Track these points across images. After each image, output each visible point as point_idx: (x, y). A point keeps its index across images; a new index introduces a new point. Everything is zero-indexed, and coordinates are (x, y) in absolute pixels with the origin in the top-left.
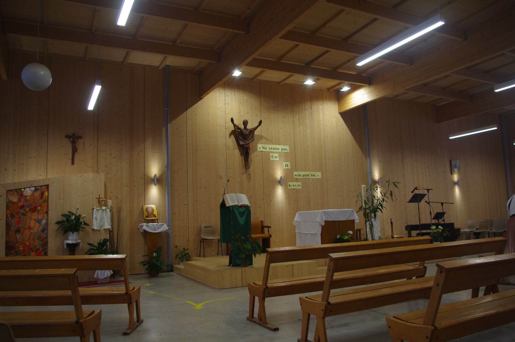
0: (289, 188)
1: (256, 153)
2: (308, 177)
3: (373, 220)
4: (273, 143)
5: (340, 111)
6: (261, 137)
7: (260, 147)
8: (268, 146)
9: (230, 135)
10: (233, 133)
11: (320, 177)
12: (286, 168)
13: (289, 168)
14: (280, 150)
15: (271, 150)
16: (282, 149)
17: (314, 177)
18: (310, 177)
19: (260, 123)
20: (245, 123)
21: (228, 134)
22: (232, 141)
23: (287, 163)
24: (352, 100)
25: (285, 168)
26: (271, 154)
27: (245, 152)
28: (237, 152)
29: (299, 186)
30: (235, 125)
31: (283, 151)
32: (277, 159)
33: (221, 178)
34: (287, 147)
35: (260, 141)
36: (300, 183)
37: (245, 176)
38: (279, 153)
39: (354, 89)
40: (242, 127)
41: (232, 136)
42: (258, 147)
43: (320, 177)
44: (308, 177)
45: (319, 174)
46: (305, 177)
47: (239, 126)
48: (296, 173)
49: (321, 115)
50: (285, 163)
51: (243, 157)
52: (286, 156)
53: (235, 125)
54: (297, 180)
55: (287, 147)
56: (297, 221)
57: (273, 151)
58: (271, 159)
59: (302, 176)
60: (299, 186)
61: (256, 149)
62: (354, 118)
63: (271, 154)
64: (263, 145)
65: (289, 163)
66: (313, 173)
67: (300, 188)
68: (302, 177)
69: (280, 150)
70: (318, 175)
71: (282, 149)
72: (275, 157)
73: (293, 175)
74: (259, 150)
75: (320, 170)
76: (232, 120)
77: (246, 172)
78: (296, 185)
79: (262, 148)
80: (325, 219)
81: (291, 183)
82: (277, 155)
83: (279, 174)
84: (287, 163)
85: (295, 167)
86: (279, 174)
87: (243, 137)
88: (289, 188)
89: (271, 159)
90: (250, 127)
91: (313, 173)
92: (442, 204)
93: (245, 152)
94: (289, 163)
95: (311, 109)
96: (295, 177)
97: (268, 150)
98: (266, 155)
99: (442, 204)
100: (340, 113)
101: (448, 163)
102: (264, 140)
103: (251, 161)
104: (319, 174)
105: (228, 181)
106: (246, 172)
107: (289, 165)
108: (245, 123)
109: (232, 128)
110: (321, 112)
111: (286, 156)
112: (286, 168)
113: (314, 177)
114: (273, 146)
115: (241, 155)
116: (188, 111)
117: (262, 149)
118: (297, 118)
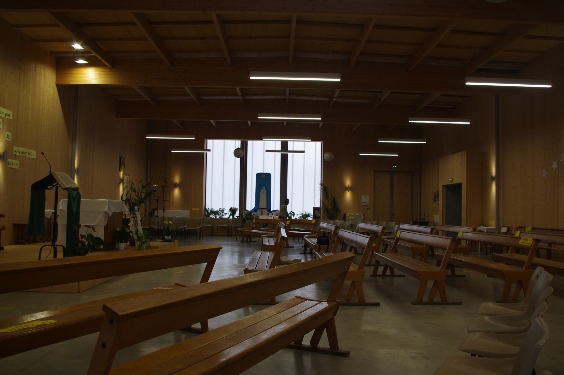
0: (9, 166)
3: (136, 213)
5: (59, 83)
13: (10, 140)
14: (4, 116)
18: (27, 155)
24: (77, 75)
29: (17, 165)
36: (18, 162)
39: (92, 63)
43: (35, 157)
45: (34, 153)
46: (22, 155)
48: (16, 148)
49: (42, 81)
50: (7, 133)
54: (16, 157)
55: (10, 113)
56: (61, 210)
60: (17, 165)
62: (71, 94)
65: (10, 134)
66: (30, 151)
67: (17, 167)
78: (14, 163)
80: (113, 210)
88: (9, 166)
92: (157, 201)
95: (35, 70)
99: (157, 201)
100: (57, 85)
101: (118, 160)
104: (34, 153)
105: (43, 153)
110: (42, 78)
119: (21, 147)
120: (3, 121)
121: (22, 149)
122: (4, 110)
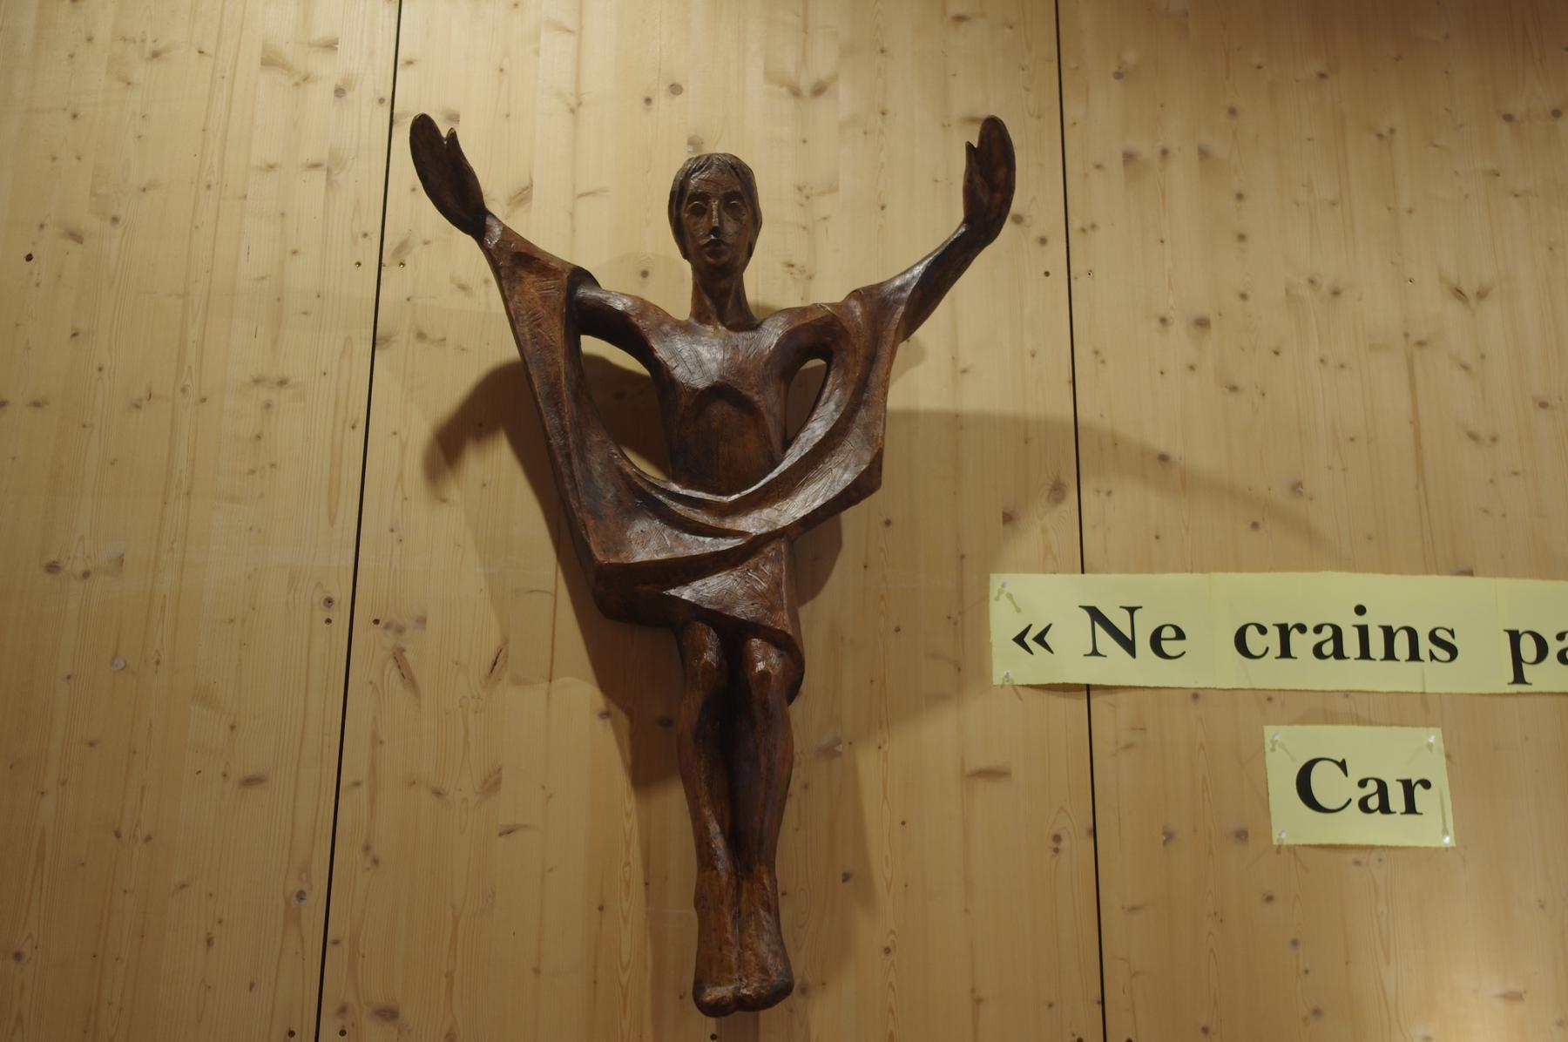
1: (938, 741)
7: (1037, 605)
8: (1209, 602)
9: (451, 443)
10: (493, 408)
15: (1269, 673)
16: (1523, 649)
19: (990, 170)
20: (714, 211)
21: (410, 422)
27: (715, 712)
28: (565, 728)
30: (515, 262)
32: (1433, 827)
35: (1050, 524)
38: (1462, 719)
40: (671, 286)
41: (496, 466)
42: (1003, 623)
47: (616, 287)
51: (674, 801)
53: (515, 262)
58: (1291, 823)
61: (963, 664)
63: (1284, 748)
69: (1483, 668)
71: (1523, 649)
74: (1011, 666)
76: (442, 167)
79: (1072, 633)
89: (1291, 823)
90: (786, 274)
93: (689, 709)
97: (1208, 664)
102: (1117, 506)
103: (855, 879)
108: (714, 211)
109: (466, 323)
114: (1324, 595)
115: (643, 776)
117: (1071, 660)
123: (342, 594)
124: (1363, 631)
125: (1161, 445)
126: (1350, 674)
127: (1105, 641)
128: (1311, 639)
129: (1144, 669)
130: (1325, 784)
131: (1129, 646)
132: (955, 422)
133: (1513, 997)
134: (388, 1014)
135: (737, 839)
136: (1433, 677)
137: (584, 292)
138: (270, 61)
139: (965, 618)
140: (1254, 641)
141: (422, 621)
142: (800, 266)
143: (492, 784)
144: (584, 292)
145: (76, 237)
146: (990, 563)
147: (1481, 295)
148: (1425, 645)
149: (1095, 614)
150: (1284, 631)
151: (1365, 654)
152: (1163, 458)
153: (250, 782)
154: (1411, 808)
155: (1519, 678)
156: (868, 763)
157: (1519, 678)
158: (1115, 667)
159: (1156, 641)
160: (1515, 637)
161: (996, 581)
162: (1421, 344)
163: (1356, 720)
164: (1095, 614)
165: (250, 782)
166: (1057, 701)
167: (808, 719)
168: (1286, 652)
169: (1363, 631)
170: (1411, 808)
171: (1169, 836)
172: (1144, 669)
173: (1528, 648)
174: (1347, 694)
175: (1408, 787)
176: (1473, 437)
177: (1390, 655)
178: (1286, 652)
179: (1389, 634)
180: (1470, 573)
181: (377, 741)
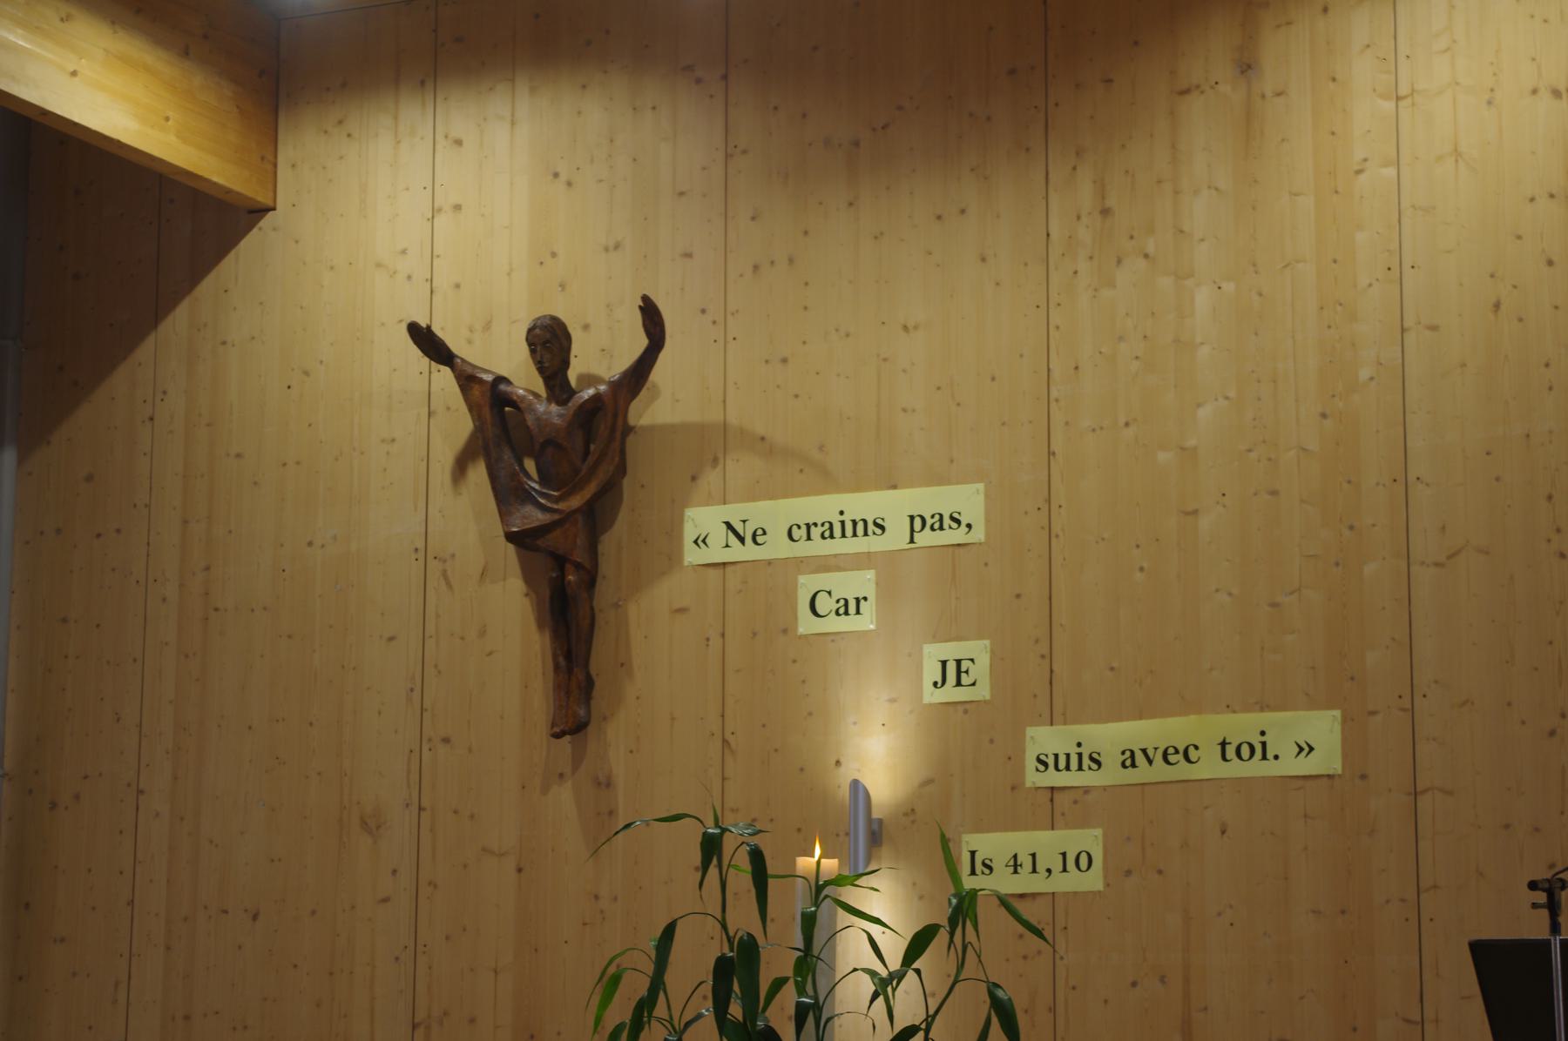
1: (665, 593)
2: (1182, 770)
4: (827, 482)
6: (707, 447)
9: (461, 466)
11: (1327, 758)
12: (950, 693)
13: (983, 692)
15: (803, 549)
16: (917, 523)
17: (1255, 768)
18: (1208, 766)
20: (550, 342)
22: (468, 518)
23: (951, 650)
25: (932, 696)
26: (807, 583)
29: (1083, 861)
30: (467, 379)
31: (925, 538)
32: (866, 621)
33: (372, 825)
34: (968, 500)
35: (711, 478)
36: (1090, 839)
37: (564, 795)
38: (885, 564)
41: (478, 474)
42: (689, 534)
43: (1327, 758)
44: (1182, 770)
48: (1045, 739)
50: (934, 653)
52: (946, 585)
53: (467, 379)
54: (1054, 808)
55: (968, 500)
57: (819, 547)
58: (807, 624)
59: (1111, 760)
60: (1083, 861)
61: (673, 556)
63: (807, 583)
64: (734, 512)
66: (1243, 725)
67: (1092, 881)
68: (1111, 774)
69: (896, 538)
70: (1310, 740)
71: (917, 523)
72: (845, 603)
73: (1014, 759)
74: (693, 556)
75: (1334, 685)
76: (426, 341)
77: (577, 761)
79: (718, 534)
81: (990, 844)
82: (861, 583)
83: (876, 754)
84: (951, 650)
85: (1042, 679)
86: (876, 754)
87: (563, 459)
89: (807, 624)
91: (1243, 725)
94: (978, 652)
95: (1246, 67)
96: (1034, 778)
97: (777, 547)
98: (764, 594)
102: (739, 467)
103: (624, 665)
106: (577, 761)
107: (980, 670)
108: (550, 342)
111: (946, 585)
112: (950, 693)
113: (1255, 768)
114: (823, 507)
116: (166, 326)
117: (715, 554)
118: (1085, 194)
119: (1115, 715)
120: (888, 590)
121: (1110, 736)
122: (891, 506)
123: (421, 545)
124: (843, 523)
125: (760, 430)
126: (839, 546)
127: (733, 539)
128: (820, 529)
129: (749, 552)
130: (824, 604)
131: (742, 540)
132: (671, 429)
133: (892, 701)
134: (446, 740)
135: (568, 656)
136: (875, 543)
137: (503, 387)
138: (379, 265)
139: (673, 531)
140: (796, 533)
141: (453, 556)
142: (599, 356)
143: (482, 633)
144: (503, 387)
145: (306, 373)
146: (686, 504)
147: (916, 328)
148: (871, 527)
149: (729, 525)
150: (808, 526)
151: (844, 535)
152: (763, 439)
153: (391, 639)
154: (858, 612)
155: (912, 541)
156: (633, 610)
157: (912, 541)
158: (738, 552)
159: (754, 536)
160: (912, 518)
161: (690, 513)
162: (885, 360)
163: (839, 569)
164: (729, 525)
165: (391, 639)
166: (712, 572)
167: (605, 592)
168: (809, 538)
169: (843, 523)
170: (858, 612)
171: (755, 634)
172: (749, 552)
173: (918, 523)
174: (835, 556)
175: (858, 600)
176: (905, 410)
177: (855, 535)
178: (809, 538)
179: (855, 523)
180: (894, 487)
181: (438, 616)
